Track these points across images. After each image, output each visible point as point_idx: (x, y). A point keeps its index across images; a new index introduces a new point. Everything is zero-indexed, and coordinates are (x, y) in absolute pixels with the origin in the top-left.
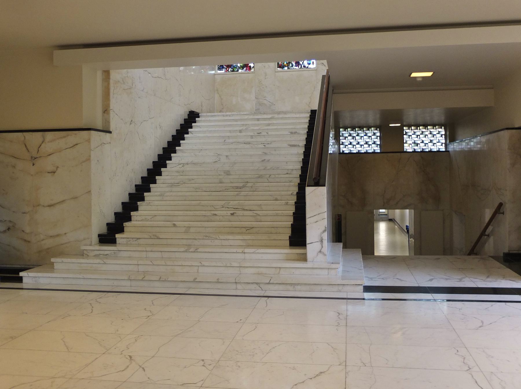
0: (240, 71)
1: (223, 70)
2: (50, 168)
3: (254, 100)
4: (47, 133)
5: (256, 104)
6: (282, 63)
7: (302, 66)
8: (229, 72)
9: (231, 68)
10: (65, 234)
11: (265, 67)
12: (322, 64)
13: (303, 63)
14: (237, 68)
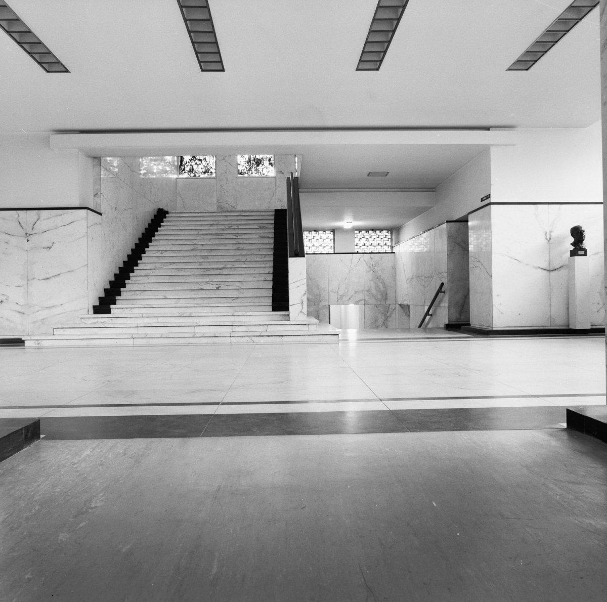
2: (45, 244)
4: (42, 211)
10: (61, 304)
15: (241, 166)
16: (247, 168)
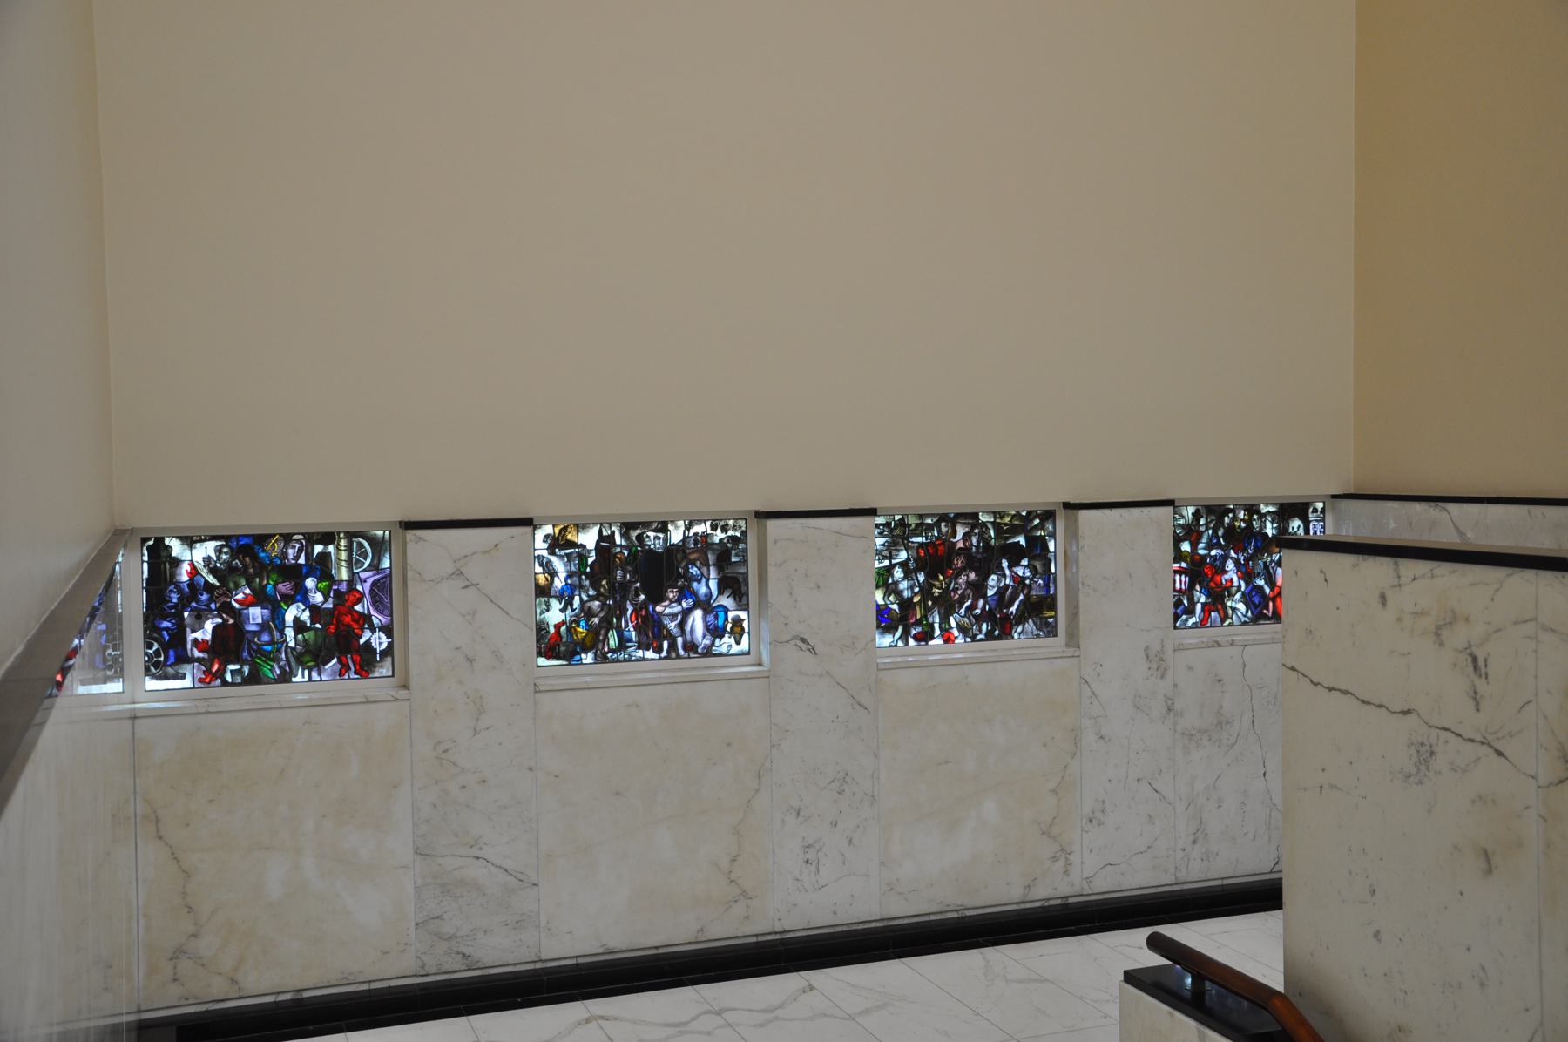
0: (300, 677)
1: (183, 677)
3: (405, 867)
5: (417, 889)
6: (563, 628)
7: (680, 641)
8: (225, 683)
9: (242, 662)
11: (470, 661)
12: (800, 644)
13: (681, 625)
14: (277, 660)
15: (556, 605)
16: (589, 614)
